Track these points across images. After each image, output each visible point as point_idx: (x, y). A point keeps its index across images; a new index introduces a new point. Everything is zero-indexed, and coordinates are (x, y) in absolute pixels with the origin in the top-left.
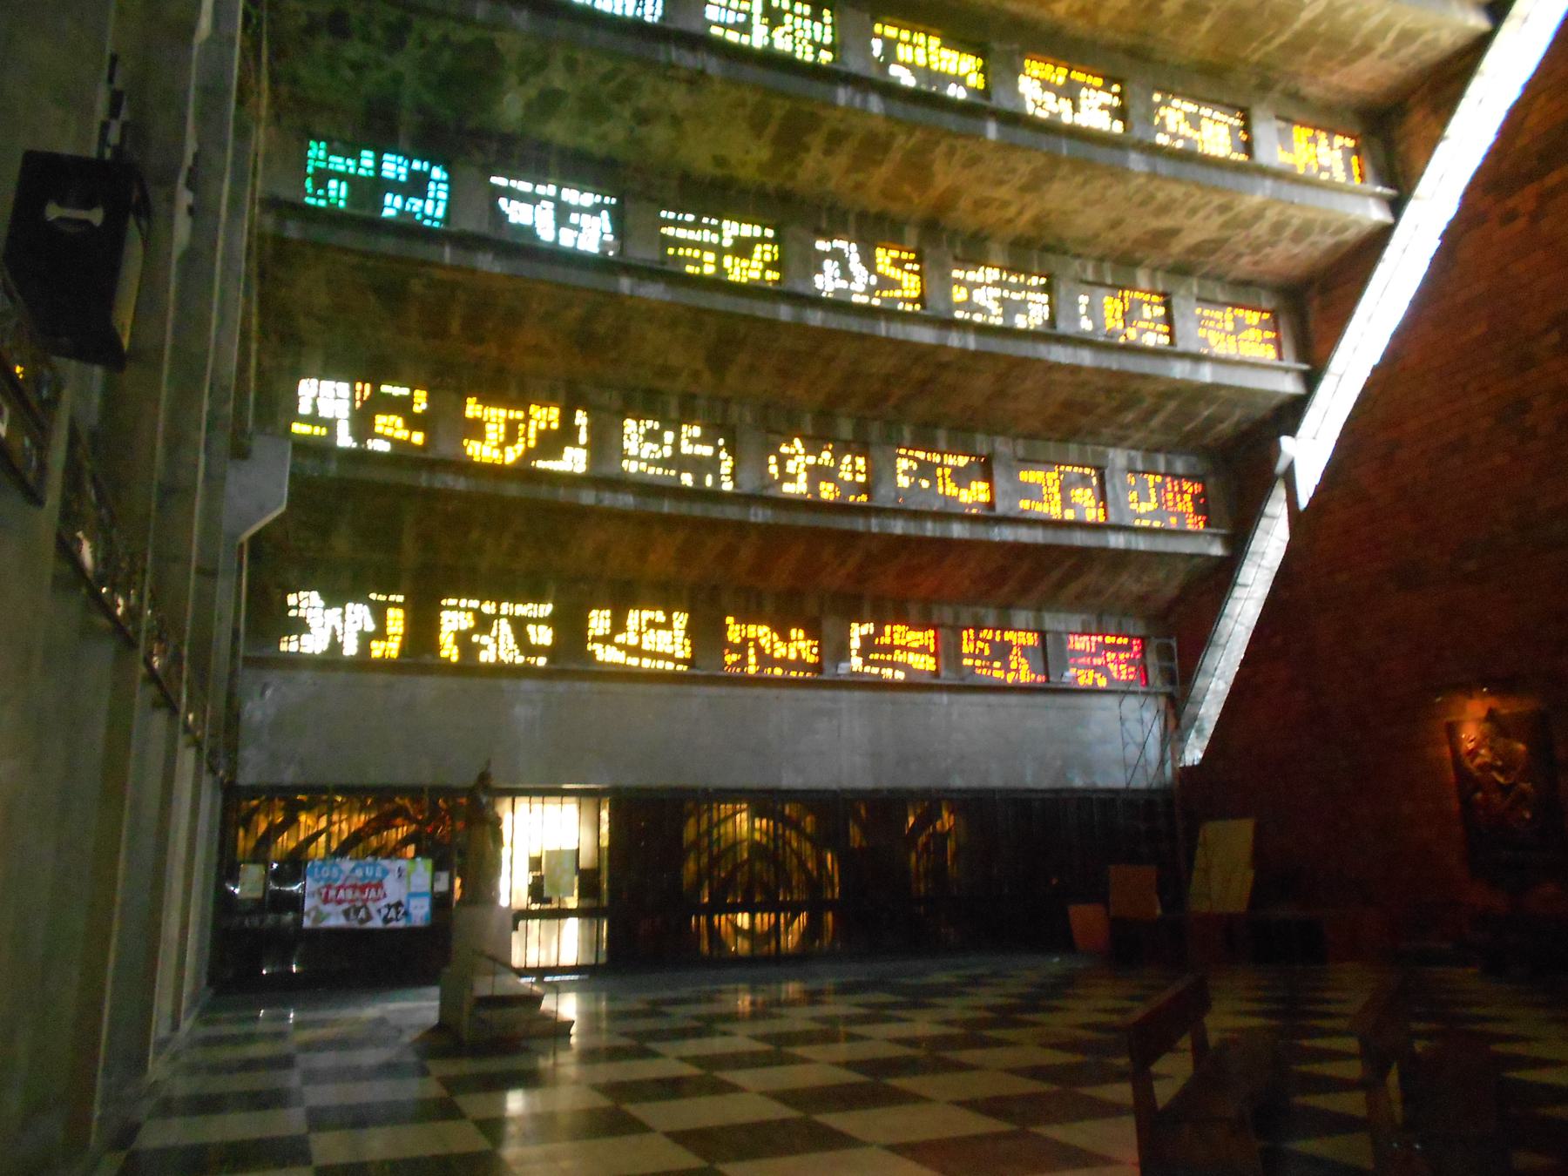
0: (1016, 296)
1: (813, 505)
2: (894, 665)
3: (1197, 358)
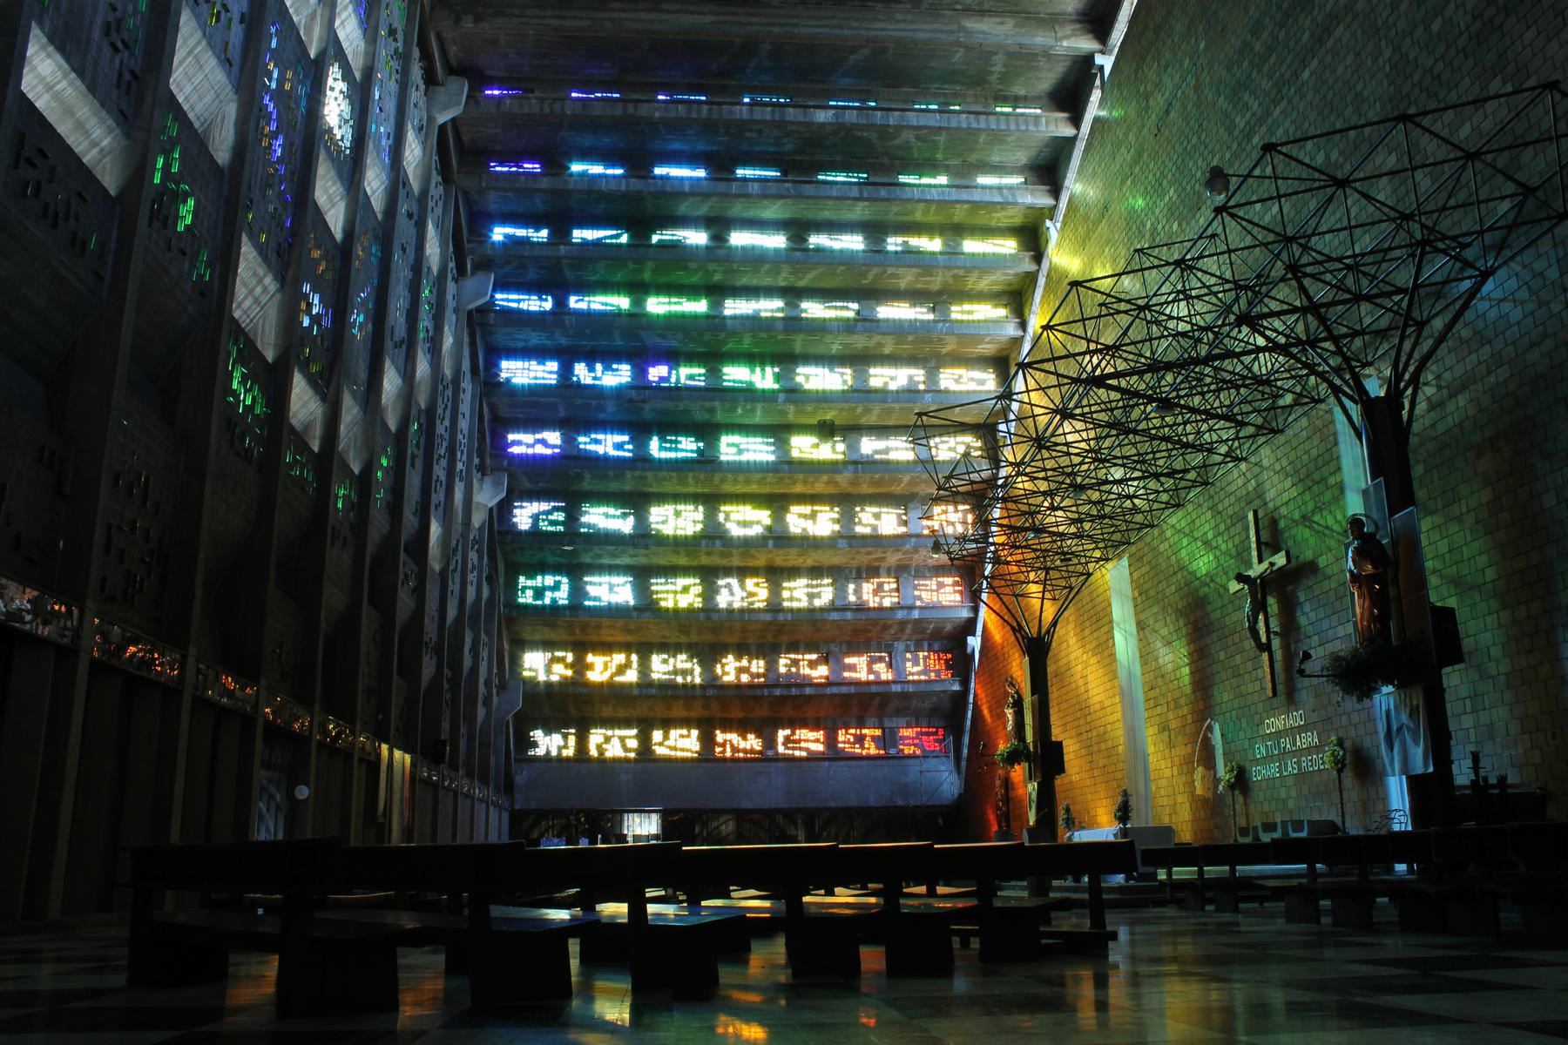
0: (815, 590)
1: (738, 686)
3: (911, 608)
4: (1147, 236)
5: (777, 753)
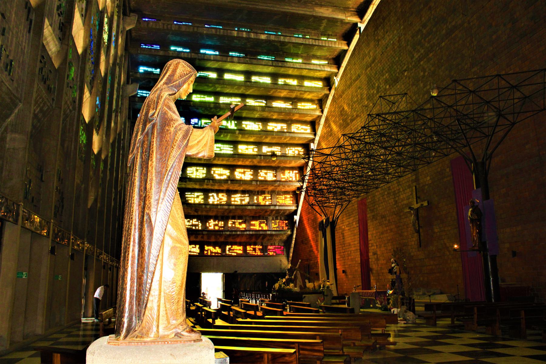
0: (243, 198)
2: (234, 252)
3: (275, 205)
4: (376, 88)
5: (226, 254)
